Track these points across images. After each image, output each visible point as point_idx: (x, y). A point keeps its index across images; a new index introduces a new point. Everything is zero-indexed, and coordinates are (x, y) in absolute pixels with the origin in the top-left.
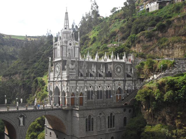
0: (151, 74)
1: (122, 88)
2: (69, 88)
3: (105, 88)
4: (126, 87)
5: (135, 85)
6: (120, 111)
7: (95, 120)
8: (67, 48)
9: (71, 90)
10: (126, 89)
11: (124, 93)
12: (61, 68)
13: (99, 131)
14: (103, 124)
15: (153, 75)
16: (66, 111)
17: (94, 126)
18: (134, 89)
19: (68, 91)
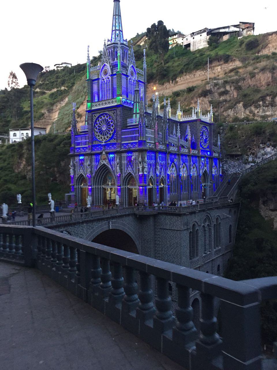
0: (259, 147)
1: (208, 172)
2: (146, 167)
3: (192, 170)
4: (213, 170)
5: (223, 167)
6: (224, 213)
7: (200, 234)
8: (127, 80)
9: (149, 173)
10: (213, 174)
11: (211, 181)
12: (119, 124)
13: (204, 257)
14: (207, 242)
15: (264, 148)
16: (141, 219)
17: (200, 248)
18: (221, 174)
19: (145, 173)
